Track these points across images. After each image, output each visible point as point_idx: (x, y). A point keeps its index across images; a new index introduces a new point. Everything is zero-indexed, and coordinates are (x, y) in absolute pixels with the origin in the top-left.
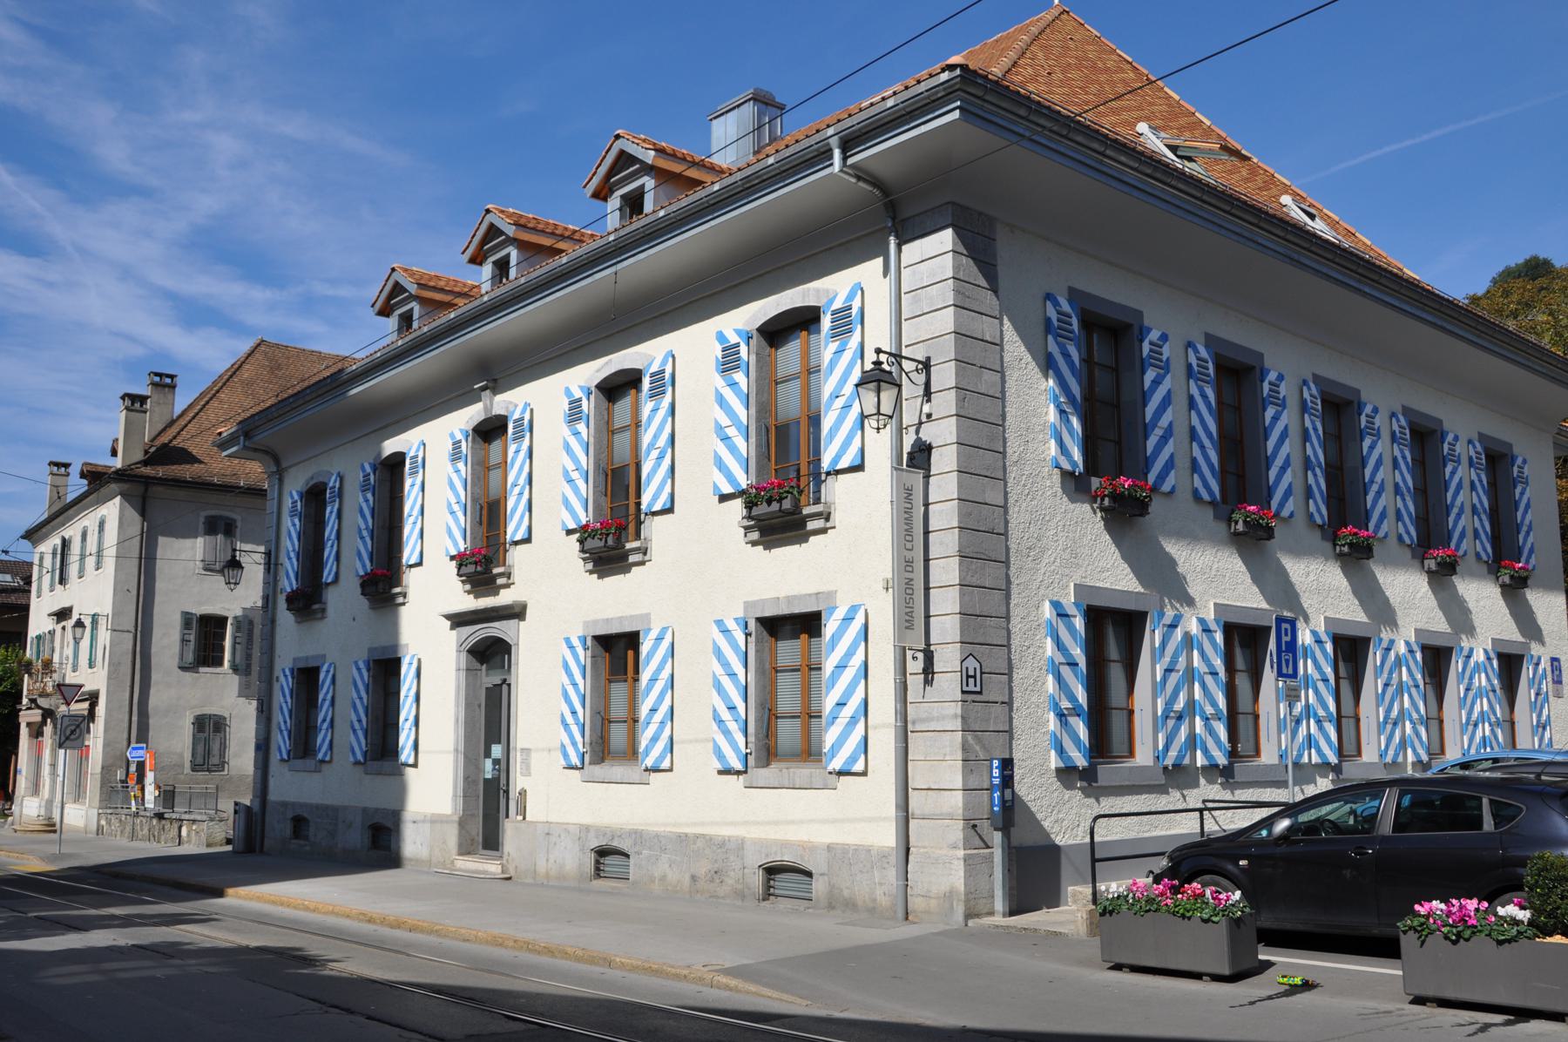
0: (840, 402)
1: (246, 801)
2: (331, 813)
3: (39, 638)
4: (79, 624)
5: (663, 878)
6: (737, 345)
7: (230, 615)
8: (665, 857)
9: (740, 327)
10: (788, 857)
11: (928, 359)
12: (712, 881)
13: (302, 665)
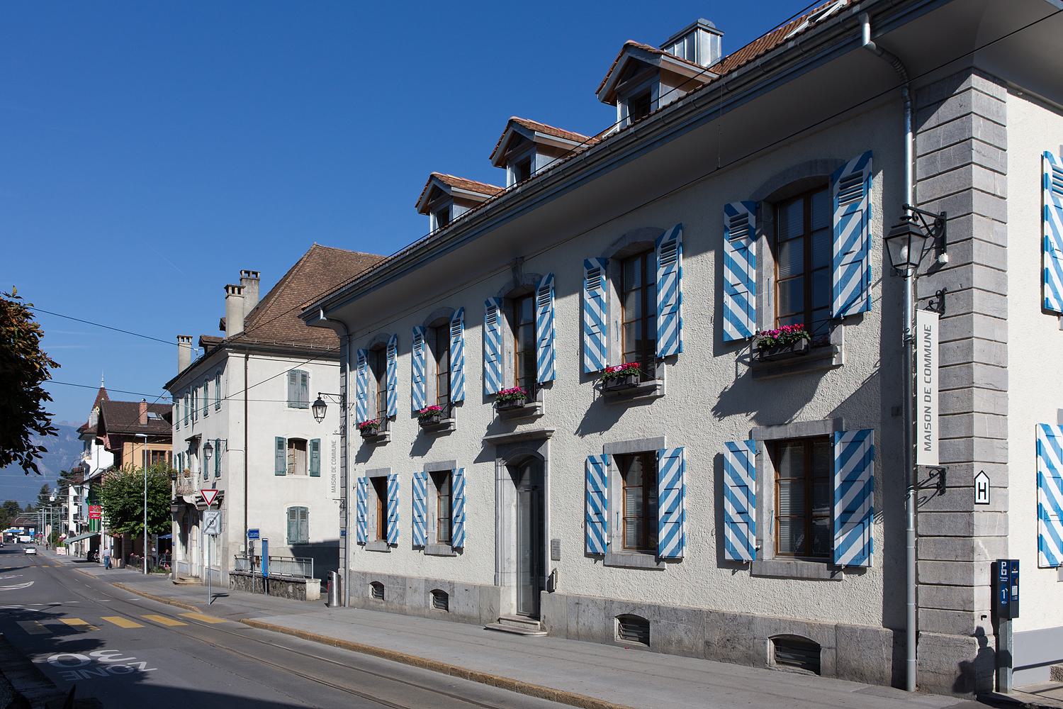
0: (849, 258)
1: (195, 527)
2: (401, 581)
3: (179, 455)
4: (208, 446)
5: (680, 642)
6: (746, 215)
7: (309, 439)
8: (681, 626)
9: (746, 199)
10: (225, 501)
11: (944, 214)
12: (725, 646)
13: (373, 475)
